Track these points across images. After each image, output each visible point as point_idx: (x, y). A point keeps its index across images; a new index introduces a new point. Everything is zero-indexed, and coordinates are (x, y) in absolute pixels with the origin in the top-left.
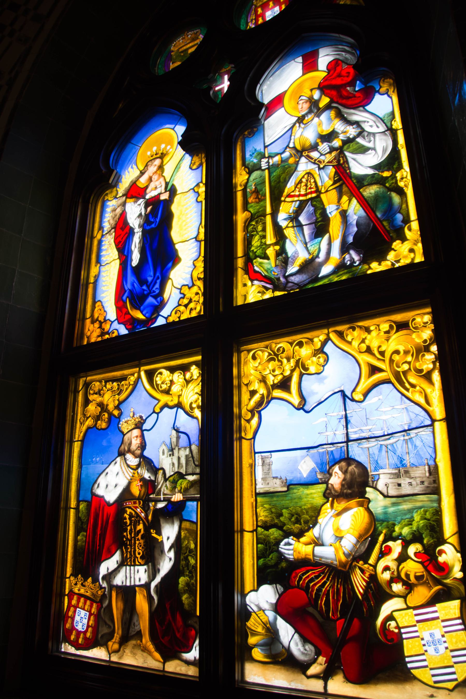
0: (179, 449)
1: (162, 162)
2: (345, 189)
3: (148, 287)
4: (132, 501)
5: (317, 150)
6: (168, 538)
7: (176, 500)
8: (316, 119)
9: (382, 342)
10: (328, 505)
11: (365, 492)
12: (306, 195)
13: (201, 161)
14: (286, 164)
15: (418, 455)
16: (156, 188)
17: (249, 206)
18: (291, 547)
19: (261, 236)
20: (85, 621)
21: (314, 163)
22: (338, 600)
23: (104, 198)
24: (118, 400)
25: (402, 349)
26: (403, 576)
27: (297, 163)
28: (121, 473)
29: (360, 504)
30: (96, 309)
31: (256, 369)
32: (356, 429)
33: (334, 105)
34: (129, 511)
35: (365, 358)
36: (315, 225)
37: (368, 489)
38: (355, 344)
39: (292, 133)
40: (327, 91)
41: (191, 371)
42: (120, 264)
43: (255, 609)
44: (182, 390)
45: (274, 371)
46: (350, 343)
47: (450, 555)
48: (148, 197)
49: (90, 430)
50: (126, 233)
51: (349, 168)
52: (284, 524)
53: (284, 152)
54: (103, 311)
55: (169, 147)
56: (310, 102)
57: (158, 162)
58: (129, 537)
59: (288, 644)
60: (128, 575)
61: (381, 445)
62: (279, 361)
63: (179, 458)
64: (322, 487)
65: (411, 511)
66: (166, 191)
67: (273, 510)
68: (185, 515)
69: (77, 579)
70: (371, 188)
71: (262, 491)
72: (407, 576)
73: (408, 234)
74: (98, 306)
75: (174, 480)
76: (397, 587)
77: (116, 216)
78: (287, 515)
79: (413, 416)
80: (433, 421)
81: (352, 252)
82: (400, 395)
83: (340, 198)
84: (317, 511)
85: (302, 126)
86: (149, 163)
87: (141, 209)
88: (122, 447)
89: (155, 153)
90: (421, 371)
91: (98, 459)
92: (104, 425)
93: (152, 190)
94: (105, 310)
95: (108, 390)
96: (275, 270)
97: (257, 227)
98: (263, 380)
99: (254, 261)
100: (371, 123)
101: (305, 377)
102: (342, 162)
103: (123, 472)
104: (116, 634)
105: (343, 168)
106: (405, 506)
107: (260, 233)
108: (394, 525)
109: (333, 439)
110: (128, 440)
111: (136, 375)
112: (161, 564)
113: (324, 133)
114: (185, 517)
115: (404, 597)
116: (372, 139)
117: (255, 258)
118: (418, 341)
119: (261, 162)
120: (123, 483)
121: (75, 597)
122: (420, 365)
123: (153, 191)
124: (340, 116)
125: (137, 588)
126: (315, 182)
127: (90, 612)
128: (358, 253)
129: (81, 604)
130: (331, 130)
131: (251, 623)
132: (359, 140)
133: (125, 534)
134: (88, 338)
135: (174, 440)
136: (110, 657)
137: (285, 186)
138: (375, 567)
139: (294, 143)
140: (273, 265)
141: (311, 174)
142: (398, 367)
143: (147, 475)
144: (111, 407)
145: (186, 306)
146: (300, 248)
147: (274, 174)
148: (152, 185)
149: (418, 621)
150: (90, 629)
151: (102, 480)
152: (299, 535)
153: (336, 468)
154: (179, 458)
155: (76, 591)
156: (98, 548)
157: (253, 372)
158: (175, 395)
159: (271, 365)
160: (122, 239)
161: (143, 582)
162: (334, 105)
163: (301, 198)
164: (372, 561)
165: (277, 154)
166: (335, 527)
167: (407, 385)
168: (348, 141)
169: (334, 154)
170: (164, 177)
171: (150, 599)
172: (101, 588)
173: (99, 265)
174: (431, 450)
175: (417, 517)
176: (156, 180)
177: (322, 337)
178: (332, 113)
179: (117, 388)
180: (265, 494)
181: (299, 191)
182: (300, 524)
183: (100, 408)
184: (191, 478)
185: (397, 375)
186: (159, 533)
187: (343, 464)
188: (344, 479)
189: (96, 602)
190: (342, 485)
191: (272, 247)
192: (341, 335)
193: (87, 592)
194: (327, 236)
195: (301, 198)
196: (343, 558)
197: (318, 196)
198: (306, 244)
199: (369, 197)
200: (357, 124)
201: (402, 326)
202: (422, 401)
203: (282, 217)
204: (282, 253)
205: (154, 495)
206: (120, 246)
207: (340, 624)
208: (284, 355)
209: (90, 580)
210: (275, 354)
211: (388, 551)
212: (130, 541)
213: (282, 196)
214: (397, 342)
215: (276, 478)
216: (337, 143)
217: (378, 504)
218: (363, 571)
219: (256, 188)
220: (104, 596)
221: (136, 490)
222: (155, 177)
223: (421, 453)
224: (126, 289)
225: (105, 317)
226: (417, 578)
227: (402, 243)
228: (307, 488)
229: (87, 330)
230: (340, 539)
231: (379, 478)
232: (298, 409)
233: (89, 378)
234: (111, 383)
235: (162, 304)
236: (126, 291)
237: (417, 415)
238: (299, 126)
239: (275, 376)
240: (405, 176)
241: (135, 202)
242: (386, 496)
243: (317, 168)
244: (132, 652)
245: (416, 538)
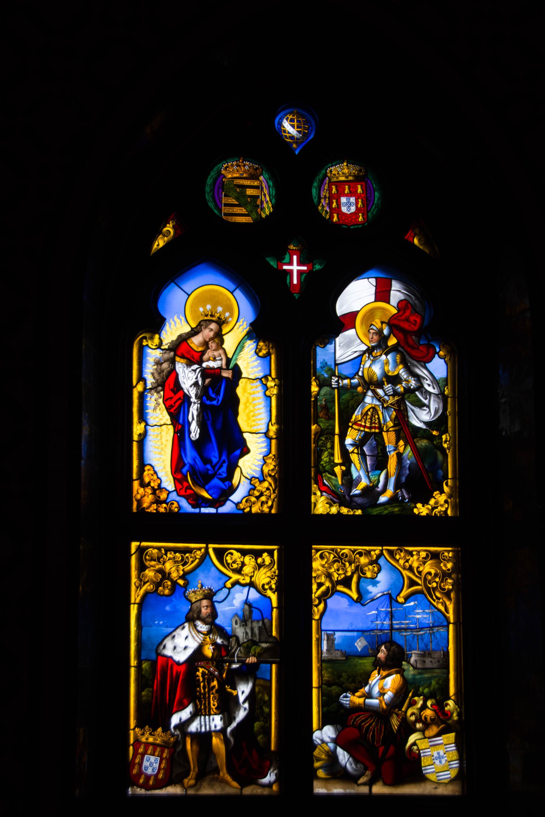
0: (252, 622)
1: (220, 330)
2: (402, 434)
3: (213, 467)
4: (205, 662)
5: (382, 388)
6: (243, 692)
7: (250, 662)
8: (384, 357)
9: (420, 565)
10: (376, 672)
11: (402, 665)
12: (370, 428)
13: (269, 350)
14: (355, 391)
15: (437, 643)
16: (215, 359)
17: (319, 420)
18: (348, 699)
19: (329, 453)
20: (156, 766)
21: (379, 400)
22: (381, 734)
23: (141, 341)
24: (183, 570)
25: (433, 572)
26: (423, 718)
27: (365, 395)
28: (190, 637)
29: (397, 673)
30: (146, 473)
31: (323, 566)
32: (398, 622)
33: (401, 349)
34: (201, 670)
35: (406, 573)
36: (377, 459)
37: (404, 663)
38: (402, 562)
39: (361, 361)
40: (395, 331)
41: (263, 557)
42: (175, 432)
43: (319, 742)
44: (254, 572)
45: (338, 570)
46: (397, 561)
48: (204, 365)
49: (149, 595)
50: (180, 399)
51: (408, 417)
52: (343, 683)
53: (353, 378)
54: (155, 477)
55: (227, 314)
56: (380, 336)
57: (213, 326)
58: (202, 691)
59: (344, 764)
60: (203, 723)
61: (414, 635)
62: (342, 563)
63: (252, 629)
64: (372, 659)
65: (430, 679)
66: (228, 369)
67: (335, 673)
68: (259, 674)
69: (144, 730)
70: (422, 441)
71: (326, 659)
72: (426, 718)
73: (446, 489)
74: (149, 470)
75: (247, 645)
76: (419, 726)
77: (163, 371)
78: (345, 677)
79: (436, 618)
80: (449, 623)
81: (403, 490)
82: (429, 603)
83: (397, 442)
84: (368, 676)
85: (372, 358)
86: (202, 323)
87: (197, 378)
88: (191, 614)
89: (210, 313)
90: (445, 589)
91: (161, 622)
92: (167, 592)
93: (208, 360)
94: (159, 476)
95: (169, 559)
96: (342, 488)
97: (327, 443)
98: (329, 576)
99: (324, 474)
100: (429, 382)
101: (361, 580)
102: (402, 408)
103: (193, 636)
104: (191, 773)
105: (403, 414)
106: (426, 675)
107: (329, 450)
108: (419, 687)
109: (381, 626)
110: (197, 608)
111: (203, 550)
112: (237, 713)
113: (390, 374)
114: (258, 676)
115: (422, 731)
116: (428, 397)
117: (324, 472)
118: (444, 568)
119: (331, 379)
120: (193, 645)
121: (142, 746)
122: (444, 586)
123: (210, 362)
124: (404, 362)
125: (213, 734)
126: (379, 418)
127: (161, 756)
128: (408, 493)
129: (149, 751)
130: (396, 373)
131: (316, 753)
132: (417, 393)
133: (198, 689)
134: (140, 502)
135: (247, 613)
136: (186, 791)
137: (353, 413)
138: (406, 712)
139: (363, 372)
140: (340, 482)
141: (376, 410)
142: (430, 584)
143: (219, 641)
144: (174, 575)
145: (258, 498)
146: (362, 473)
147: (344, 397)
148: (209, 354)
149: (431, 746)
150: (162, 772)
151: (169, 643)
152: (353, 692)
153: (383, 648)
154: (252, 629)
155: (143, 740)
156: (168, 702)
157: (320, 568)
158: (247, 575)
159: (335, 566)
160: (175, 403)
161: (219, 728)
162: (401, 349)
163: (366, 430)
164: (403, 709)
165: (346, 378)
166: (381, 686)
167: (434, 597)
168: (409, 391)
169: (396, 398)
170: (224, 350)
171: (226, 741)
172: (173, 735)
173: (143, 425)
174: (445, 642)
175: (434, 683)
176: (213, 348)
177: (377, 552)
178: (398, 358)
179: (180, 558)
180: (329, 661)
181: (365, 422)
182: (356, 683)
183: (160, 576)
184: (264, 645)
185: (428, 589)
186: (235, 689)
187: (388, 644)
188: (388, 655)
189: (168, 748)
190: (387, 658)
191: (339, 467)
192: (391, 553)
193: (157, 740)
194: (384, 472)
195: (366, 430)
196: (384, 706)
197: (380, 433)
198: (368, 472)
199: (420, 448)
200: (418, 378)
201: (435, 556)
202: (443, 609)
203: (348, 441)
204: (347, 474)
205: (228, 658)
206: (172, 410)
207: (381, 750)
208: (347, 559)
209: (160, 730)
210: (339, 557)
211: (415, 703)
212: (204, 694)
213: (350, 421)
215: (338, 650)
216: (400, 388)
217: (410, 672)
218: (398, 715)
219: (326, 404)
220: (176, 743)
222: (213, 345)
223: (439, 643)
224: (186, 462)
225: (159, 485)
226: (430, 719)
227: (441, 494)
228: (361, 659)
229: (135, 492)
230: (382, 694)
231: (411, 656)
232: (356, 602)
233: (144, 544)
234: (173, 553)
235: (232, 490)
236: (185, 465)
237: (439, 618)
238: (369, 357)
239: (339, 575)
240: (448, 439)
241: (189, 365)
242: (415, 668)
243: (381, 407)
244: (209, 784)
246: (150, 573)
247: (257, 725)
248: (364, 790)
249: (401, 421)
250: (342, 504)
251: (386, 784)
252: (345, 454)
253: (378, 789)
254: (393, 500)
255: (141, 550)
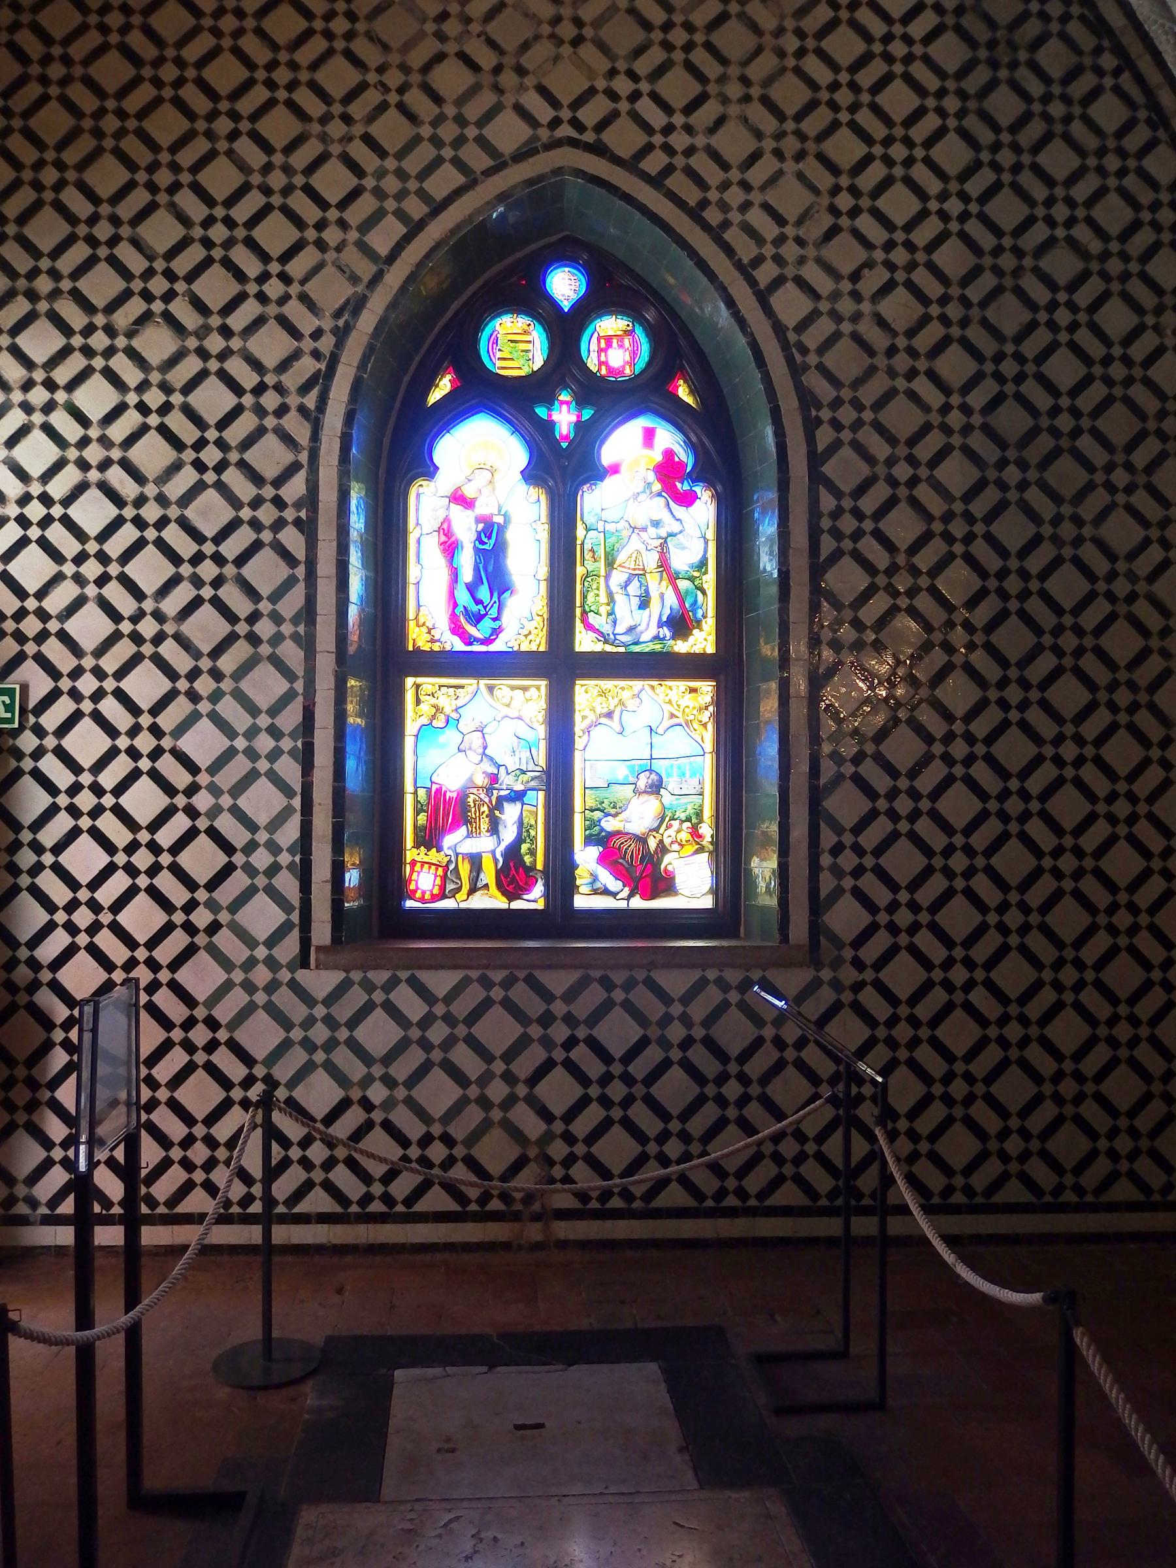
35: (667, 708)
47: (707, 830)
144: (448, 710)
171: (496, 861)
201: (693, 690)
204: (611, 613)
214: (689, 700)
221: (481, 780)
233: (419, 680)
245: (689, 819)
246: (426, 708)
247: (524, 848)
248: (622, 905)
249: (664, 564)
250: (606, 642)
251: (645, 897)
252: (610, 595)
253: (637, 903)
254: (657, 638)
255: (418, 687)
